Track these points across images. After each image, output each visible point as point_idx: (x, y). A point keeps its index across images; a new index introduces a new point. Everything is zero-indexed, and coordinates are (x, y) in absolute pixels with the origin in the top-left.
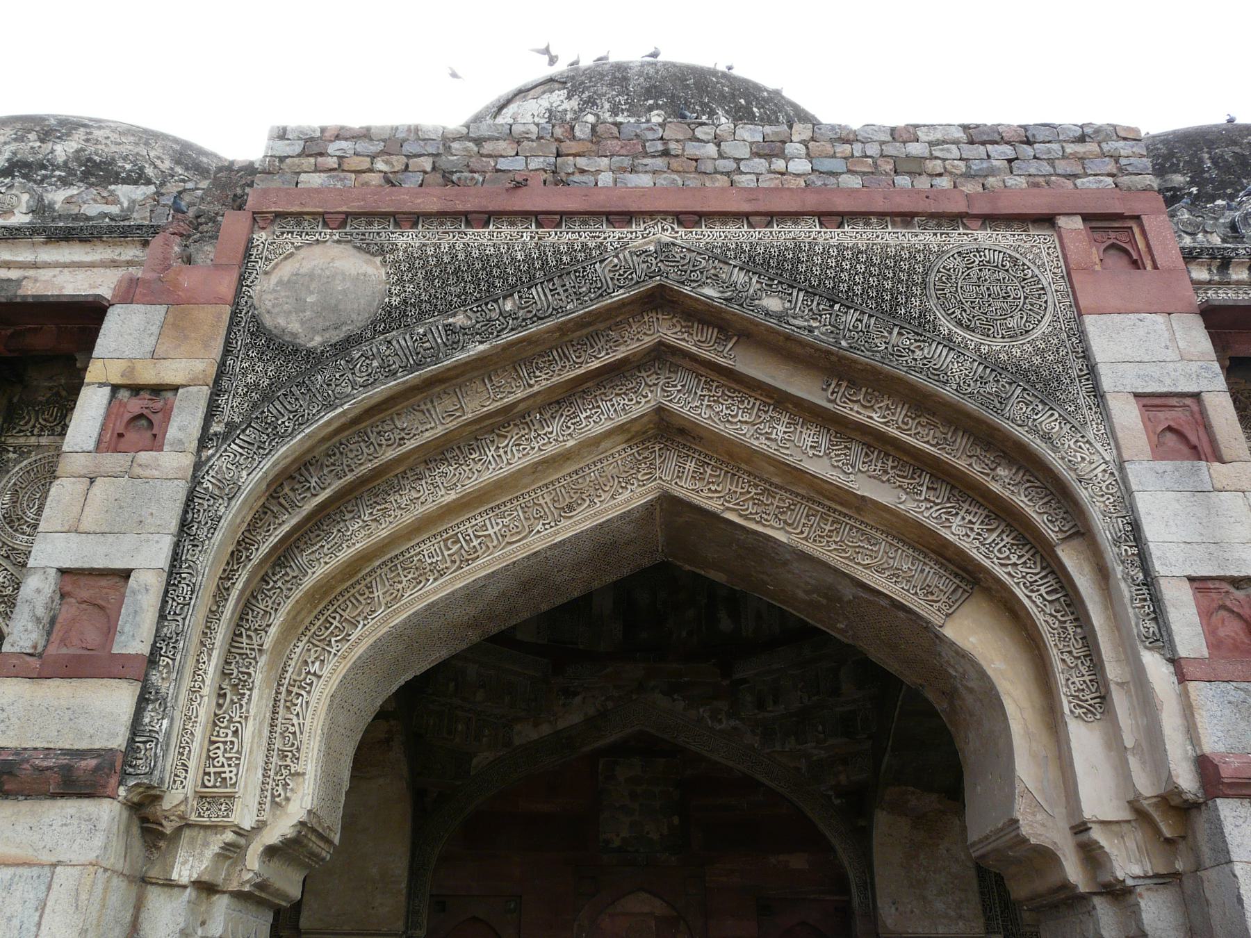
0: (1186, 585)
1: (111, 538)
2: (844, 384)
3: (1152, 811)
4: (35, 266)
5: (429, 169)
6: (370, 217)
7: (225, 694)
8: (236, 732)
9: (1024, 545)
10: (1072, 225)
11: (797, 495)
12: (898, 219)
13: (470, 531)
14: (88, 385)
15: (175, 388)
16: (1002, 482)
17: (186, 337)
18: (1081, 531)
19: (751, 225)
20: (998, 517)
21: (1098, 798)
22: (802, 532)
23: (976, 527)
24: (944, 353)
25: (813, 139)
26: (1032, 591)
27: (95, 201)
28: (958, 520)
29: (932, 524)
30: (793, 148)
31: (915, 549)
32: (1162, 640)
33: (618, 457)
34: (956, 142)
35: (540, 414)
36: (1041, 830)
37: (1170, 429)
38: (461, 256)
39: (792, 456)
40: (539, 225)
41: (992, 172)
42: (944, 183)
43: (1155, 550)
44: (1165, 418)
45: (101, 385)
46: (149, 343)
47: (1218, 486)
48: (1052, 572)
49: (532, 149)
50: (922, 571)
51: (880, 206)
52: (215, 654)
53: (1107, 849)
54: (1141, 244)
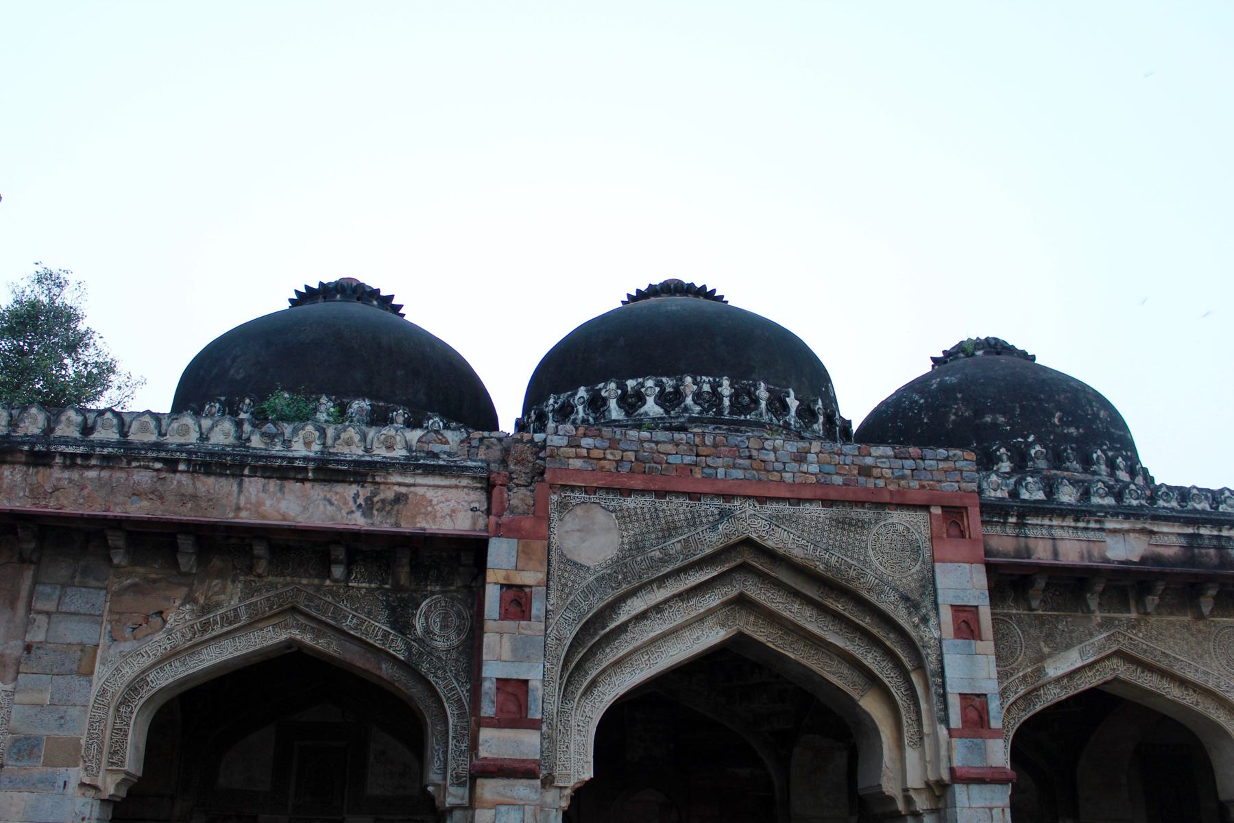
4: (414, 485)
10: (936, 511)
15: (530, 587)
16: (890, 641)
17: (531, 559)
18: (920, 666)
21: (914, 779)
29: (859, 657)
30: (812, 457)
32: (945, 720)
34: (887, 457)
39: (801, 622)
40: (690, 499)
41: (903, 477)
42: (881, 483)
43: (948, 681)
44: (963, 616)
46: (514, 559)
51: (850, 497)
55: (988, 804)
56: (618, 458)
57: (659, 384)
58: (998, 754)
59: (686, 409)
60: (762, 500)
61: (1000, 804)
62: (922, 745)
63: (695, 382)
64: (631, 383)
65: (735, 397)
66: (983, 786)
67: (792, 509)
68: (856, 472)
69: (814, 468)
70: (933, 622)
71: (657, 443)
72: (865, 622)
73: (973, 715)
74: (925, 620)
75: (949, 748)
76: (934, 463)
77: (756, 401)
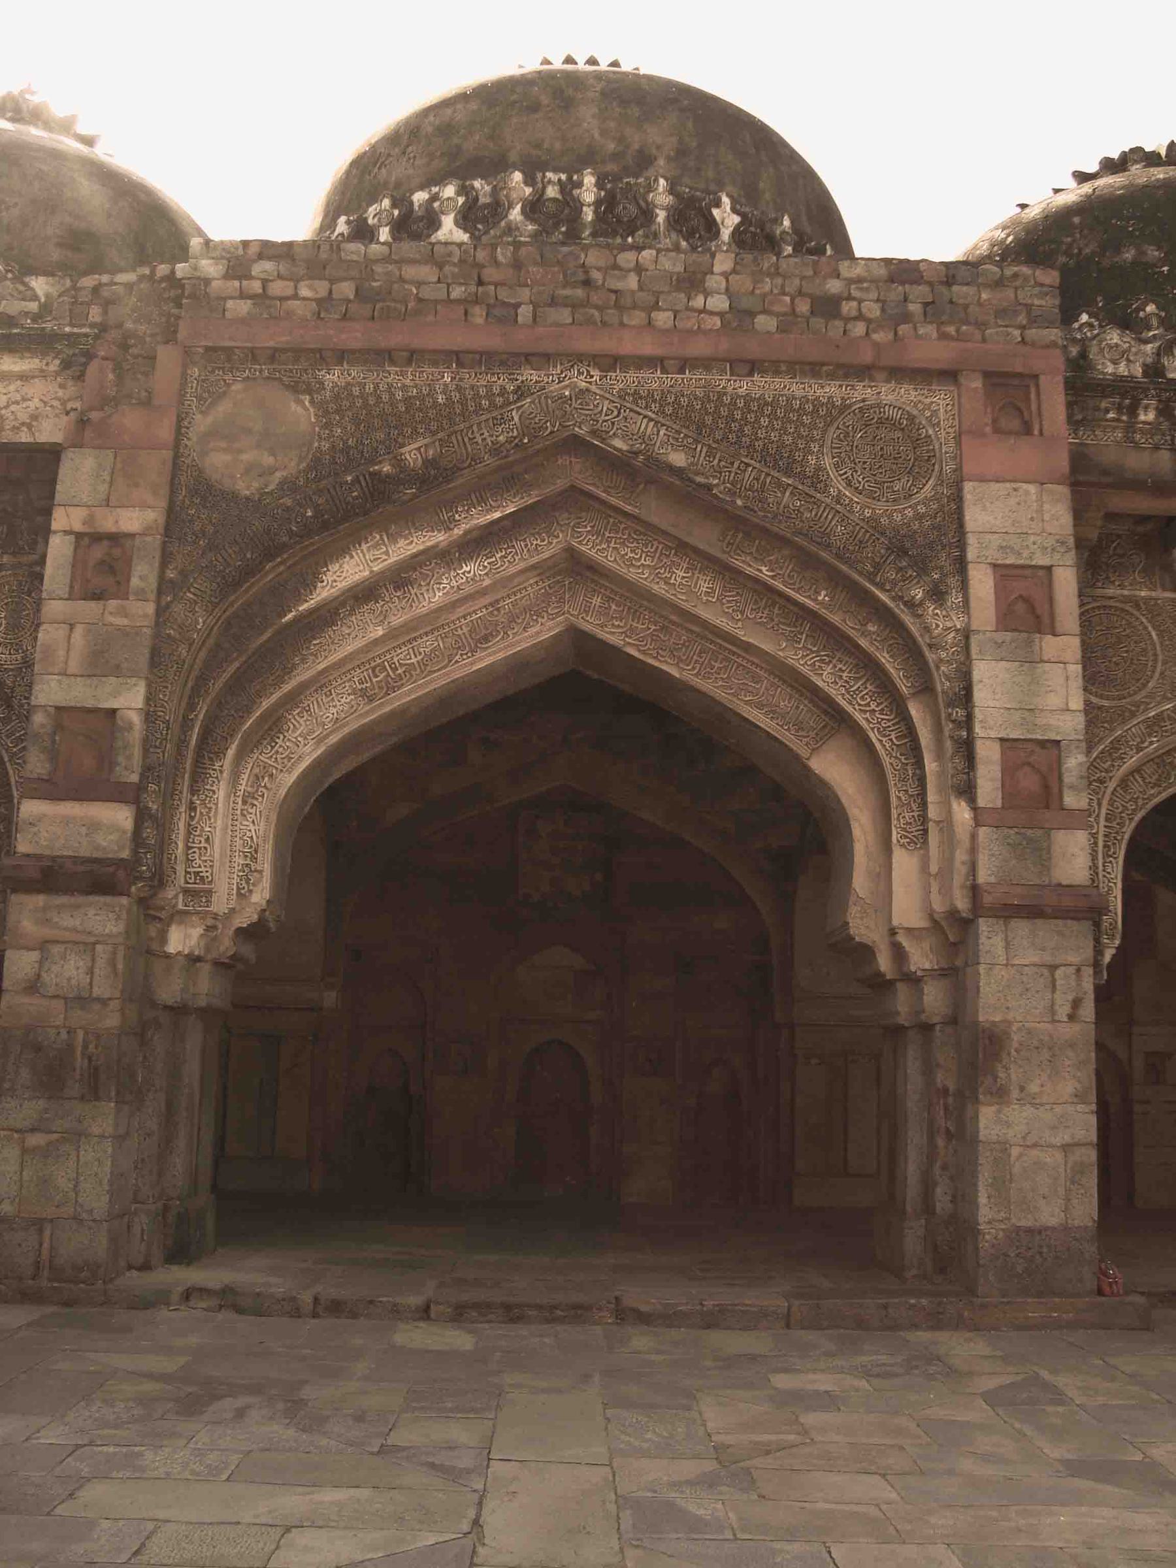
0: (997, 746)
1: (95, 680)
2: (740, 535)
3: (943, 923)
5: (352, 297)
6: (298, 352)
7: (195, 809)
8: (207, 840)
9: (884, 693)
11: (692, 632)
12: (807, 368)
13: (395, 660)
14: (55, 532)
15: (132, 536)
17: (137, 485)
18: (926, 688)
19: (664, 371)
20: (865, 667)
21: (907, 909)
22: (694, 668)
23: (845, 674)
24: (830, 517)
25: (734, 271)
26: (885, 736)
27: (12, 296)
28: (829, 669)
29: (805, 670)
30: (715, 282)
31: (792, 686)
32: (967, 791)
33: (532, 588)
35: (460, 554)
36: (863, 931)
37: (1021, 596)
38: (385, 397)
40: (460, 364)
43: (978, 714)
45: (66, 532)
46: (103, 488)
47: (1046, 658)
48: (904, 719)
49: (453, 274)
50: (797, 707)
52: (187, 776)
53: (907, 949)
54: (1034, 407)
55: (1048, 959)
56: (323, 293)
57: (463, 190)
58: (1074, 857)
59: (510, 229)
60: (611, 362)
61: (1074, 958)
62: (925, 842)
63: (529, 180)
64: (420, 197)
65: (607, 205)
66: (1039, 922)
67: (669, 379)
68: (803, 307)
69: (719, 302)
70: (955, 598)
71: (400, 262)
72: (819, 600)
73: (1029, 782)
74: (937, 595)
75: (973, 850)
76: (970, 290)
77: (648, 214)
